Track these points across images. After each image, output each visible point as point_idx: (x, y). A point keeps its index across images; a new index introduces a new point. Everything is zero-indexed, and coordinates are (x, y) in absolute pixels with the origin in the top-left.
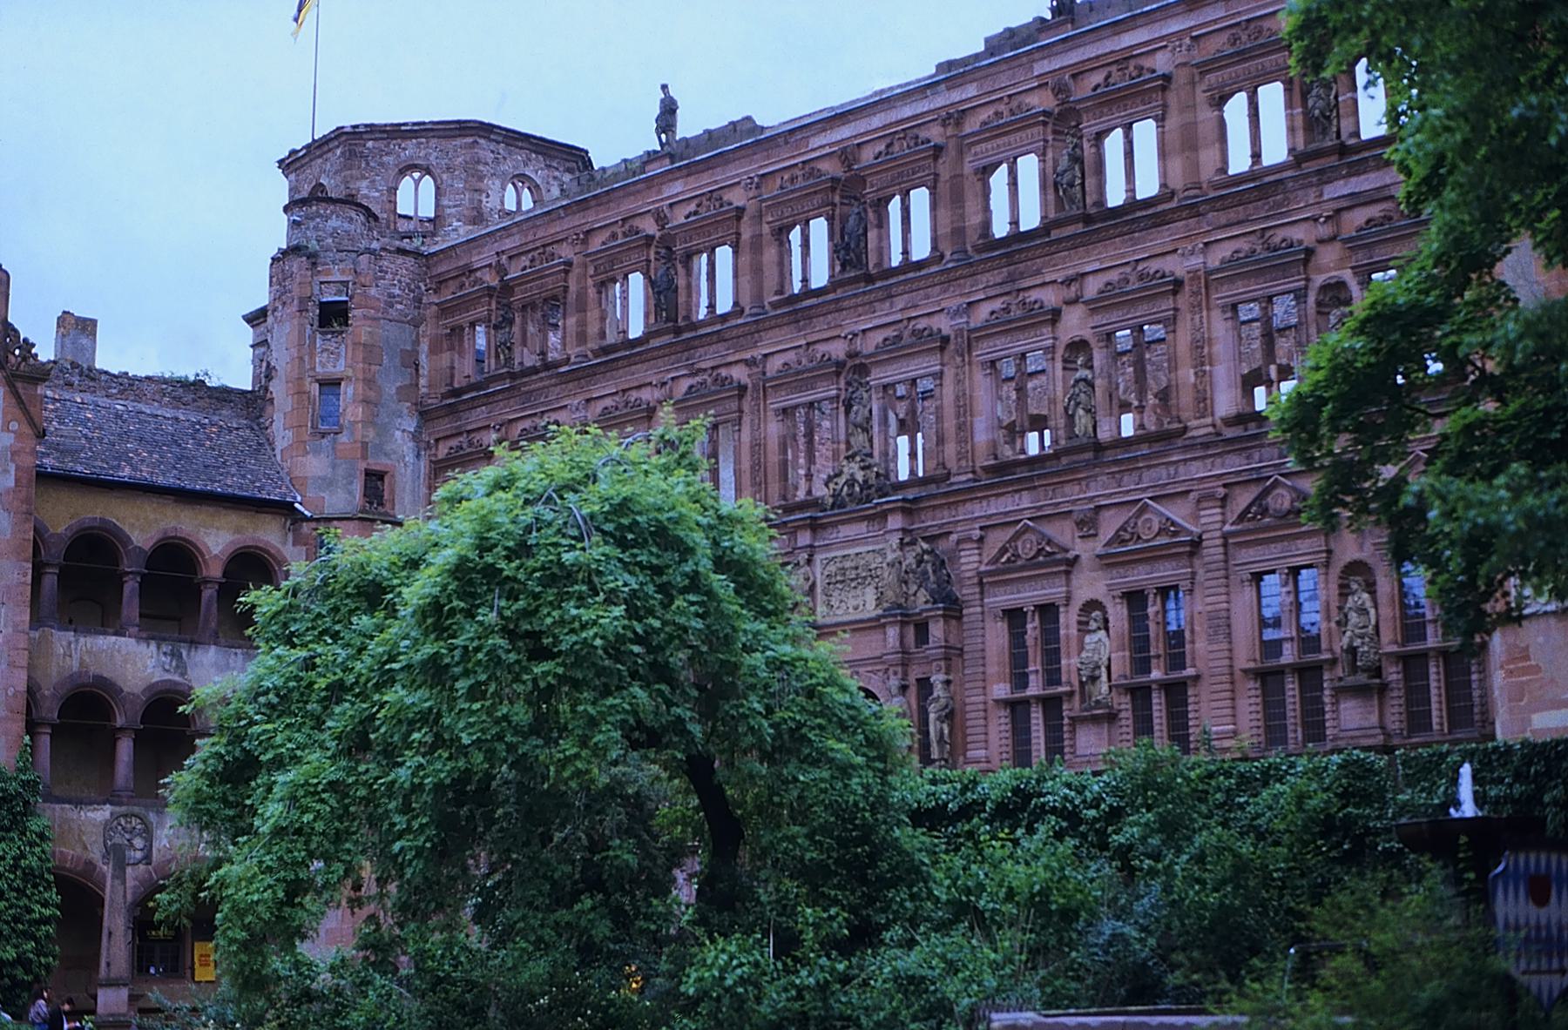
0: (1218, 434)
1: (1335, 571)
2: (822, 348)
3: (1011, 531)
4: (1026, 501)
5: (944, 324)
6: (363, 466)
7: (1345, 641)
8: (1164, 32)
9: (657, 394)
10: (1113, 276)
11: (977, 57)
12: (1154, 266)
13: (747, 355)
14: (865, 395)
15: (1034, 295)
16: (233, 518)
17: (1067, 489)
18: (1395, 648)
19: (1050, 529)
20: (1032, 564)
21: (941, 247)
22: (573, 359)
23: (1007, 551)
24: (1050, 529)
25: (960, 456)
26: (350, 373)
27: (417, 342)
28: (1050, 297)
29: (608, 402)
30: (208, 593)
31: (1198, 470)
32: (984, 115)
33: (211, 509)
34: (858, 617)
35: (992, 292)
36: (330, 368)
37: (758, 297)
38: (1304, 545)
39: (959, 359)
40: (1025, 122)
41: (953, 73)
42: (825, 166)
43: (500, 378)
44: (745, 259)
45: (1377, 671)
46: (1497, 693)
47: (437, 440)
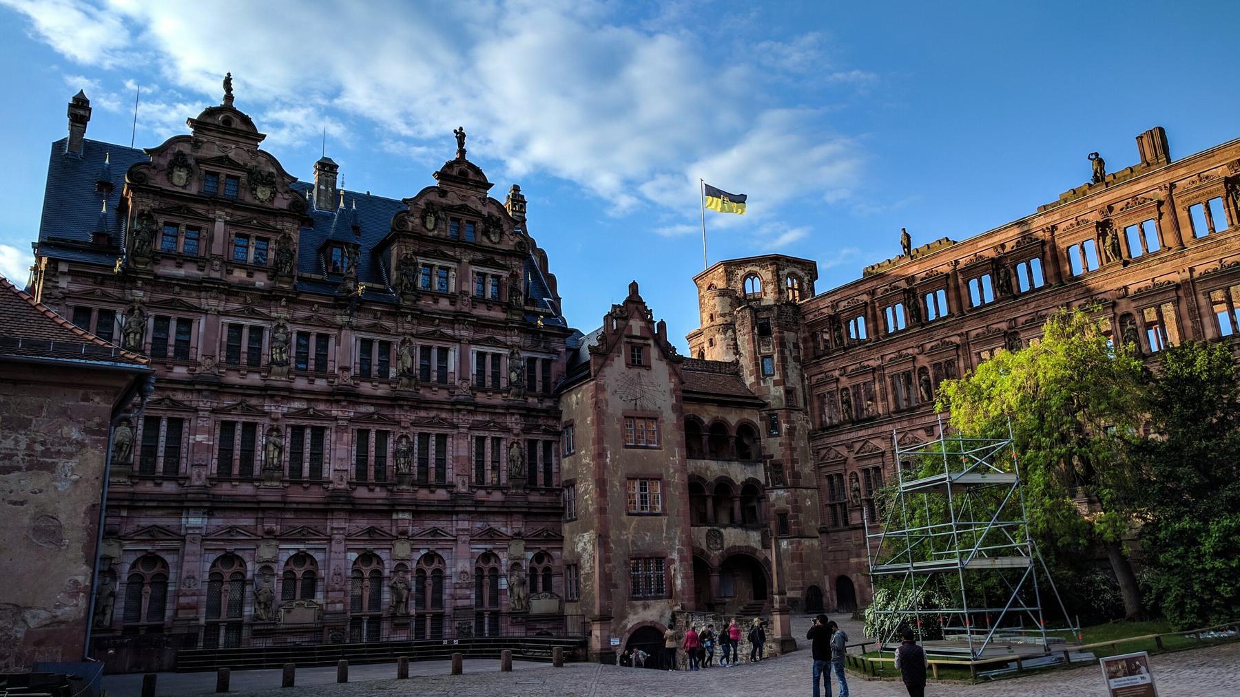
2: (995, 326)
30: (732, 441)
37: (960, 308)
44: (952, 294)
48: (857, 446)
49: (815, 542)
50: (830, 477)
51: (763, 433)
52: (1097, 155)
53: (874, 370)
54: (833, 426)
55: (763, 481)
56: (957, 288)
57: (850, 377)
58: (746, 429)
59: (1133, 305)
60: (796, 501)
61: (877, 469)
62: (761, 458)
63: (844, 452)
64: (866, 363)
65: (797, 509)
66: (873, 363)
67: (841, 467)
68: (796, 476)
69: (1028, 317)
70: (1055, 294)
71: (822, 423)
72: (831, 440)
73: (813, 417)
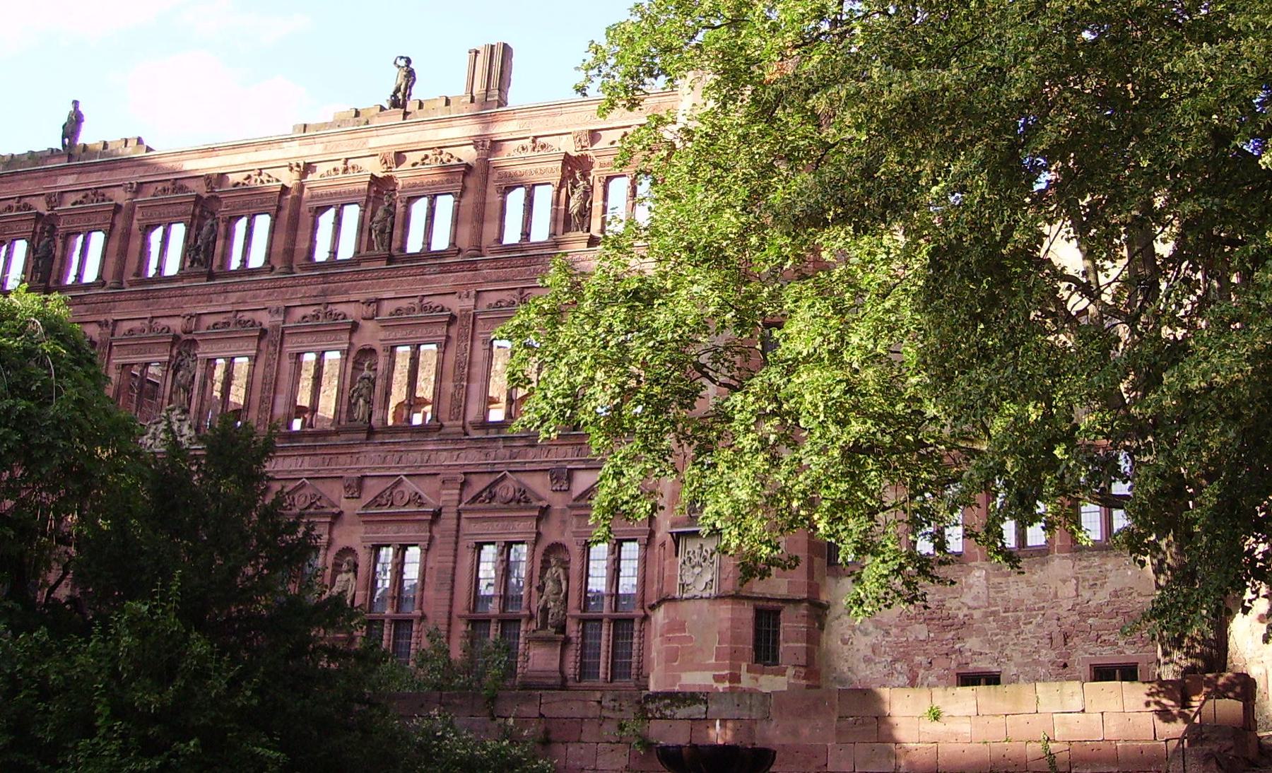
0: (466, 434)
1: (540, 550)
2: (164, 322)
4: (307, 463)
7: (542, 602)
12: (436, 301)
13: (102, 319)
15: (340, 308)
17: (342, 459)
18: (578, 613)
21: (273, 262)
28: (352, 311)
31: (444, 458)
35: (306, 302)
37: (120, 274)
38: (521, 526)
42: (191, 185)
44: (115, 244)
45: (562, 628)
46: (654, 654)
52: (408, 61)
56: (127, 235)
59: (382, 335)
69: (220, 319)
70: (275, 286)
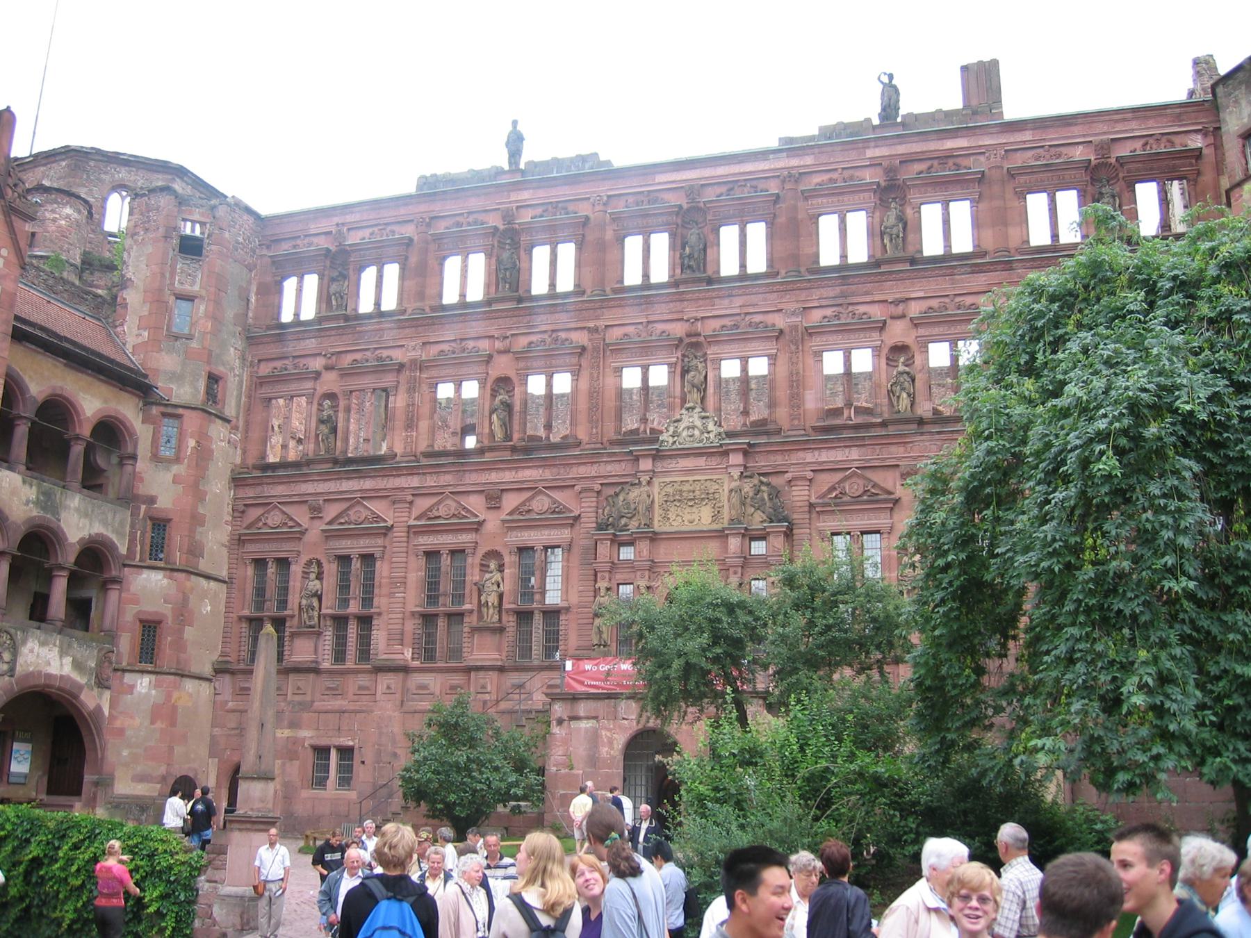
3: (839, 476)
4: (855, 454)
5: (780, 321)
6: (208, 369)
8: (981, 143)
9: (498, 345)
10: (934, 303)
11: (812, 138)
14: (700, 366)
15: (861, 309)
16: (104, 389)
17: (893, 449)
19: (877, 477)
20: (856, 500)
22: (409, 311)
23: (835, 489)
24: (877, 477)
25: (793, 417)
26: (203, 293)
27: (249, 283)
28: (877, 312)
29: (445, 347)
30: (77, 450)
32: (817, 179)
33: (90, 379)
34: (694, 528)
36: (187, 287)
39: (793, 347)
40: (862, 188)
41: (791, 147)
43: (336, 318)
47: (260, 361)
48: (332, 511)
49: (205, 689)
50: (260, 563)
51: (143, 449)
52: (891, 77)
53: (401, 367)
54: (283, 465)
55: (123, 549)
57: (345, 373)
58: (109, 432)
59: (914, 333)
60: (185, 599)
61: (368, 559)
62: (129, 499)
63: (301, 516)
64: (385, 353)
65: (184, 614)
66: (398, 356)
67: (287, 546)
68: (195, 550)
71: (263, 456)
72: (279, 490)
73: (246, 438)
